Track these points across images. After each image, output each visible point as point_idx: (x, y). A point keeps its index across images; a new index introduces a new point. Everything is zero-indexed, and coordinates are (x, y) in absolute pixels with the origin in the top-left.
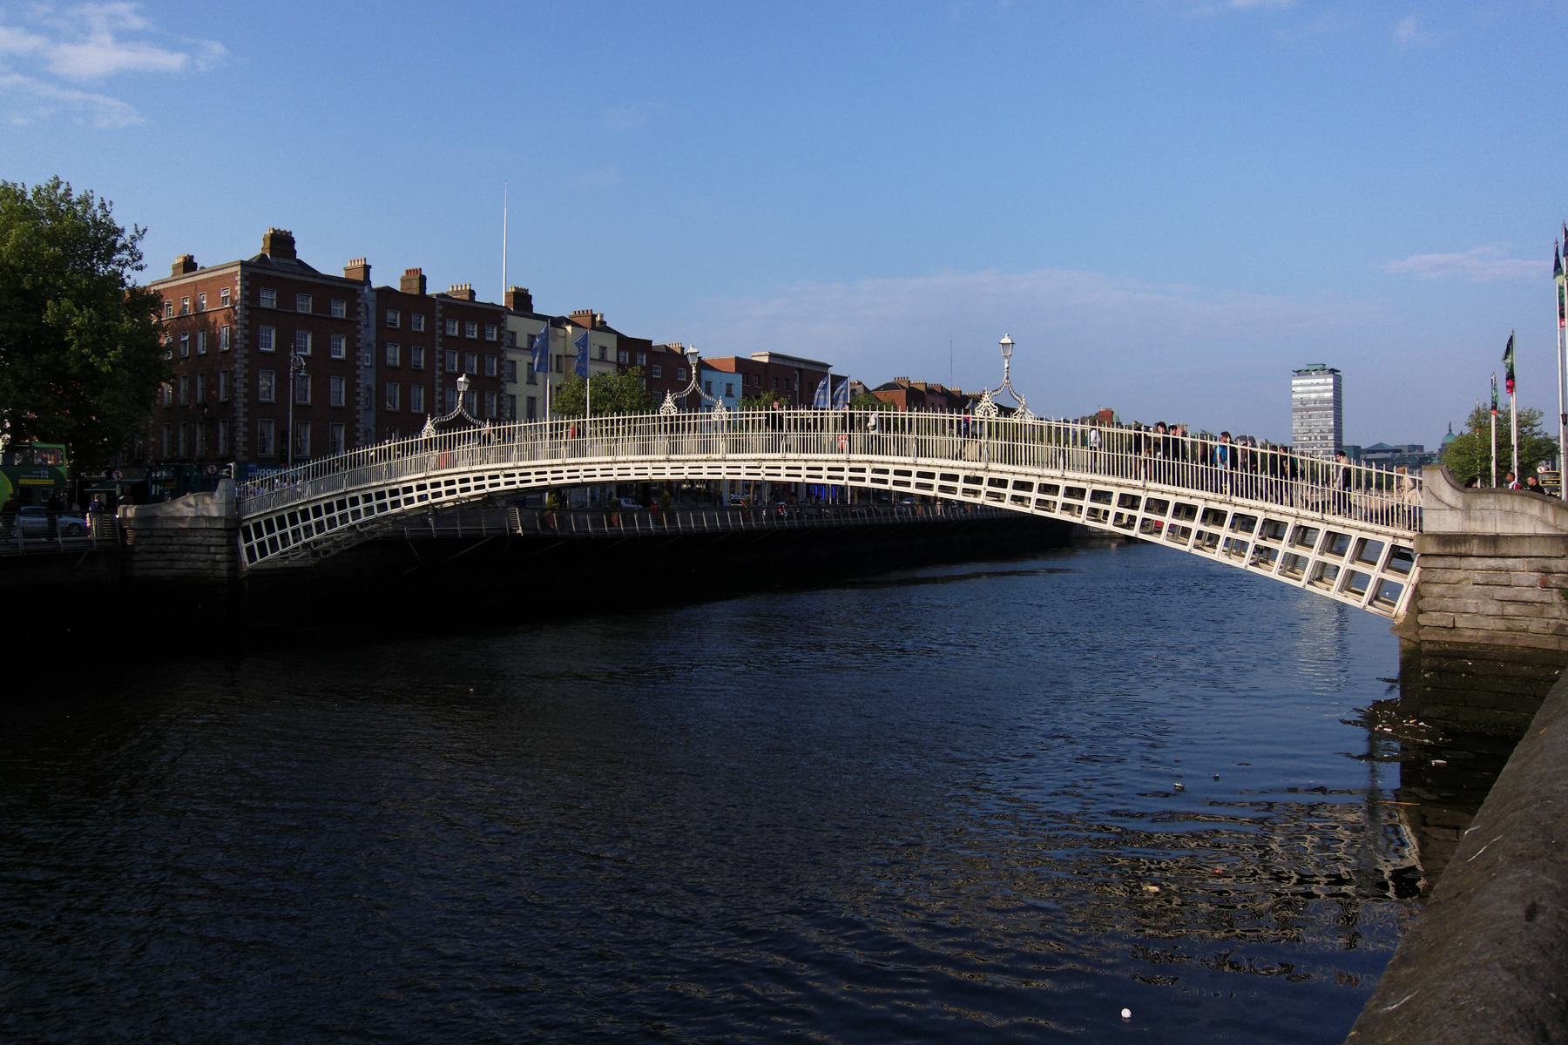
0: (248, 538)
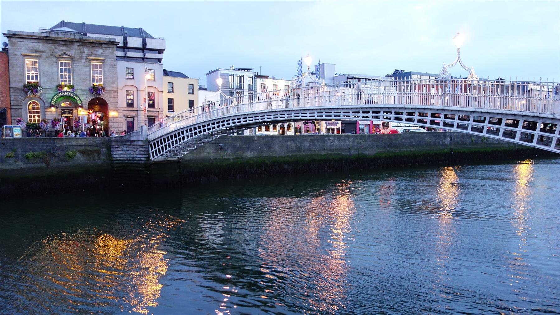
0: (152, 149)
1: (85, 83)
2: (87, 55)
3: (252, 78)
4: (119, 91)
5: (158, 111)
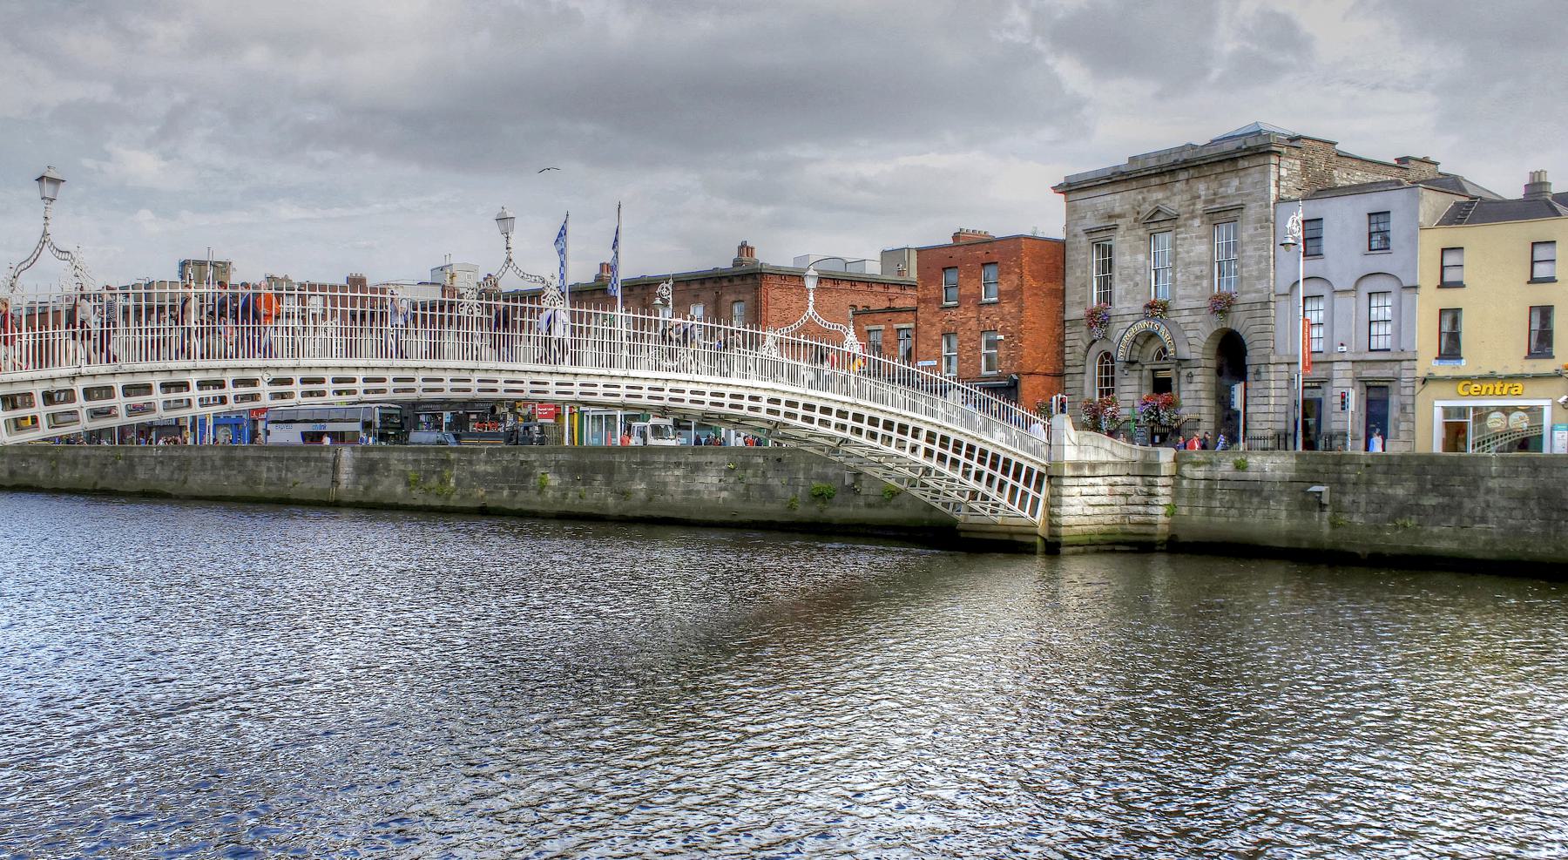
1: (1199, 288)
2: (1206, 202)
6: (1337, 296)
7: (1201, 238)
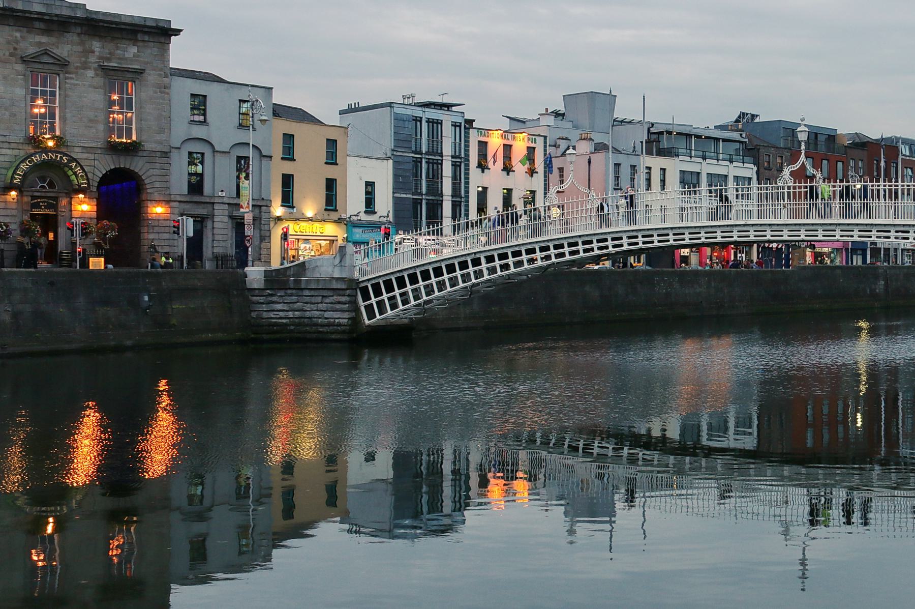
0: (366, 297)
3: (460, 127)
4: (174, 155)
5: (260, 206)
6: (218, 155)
7: (95, 88)
